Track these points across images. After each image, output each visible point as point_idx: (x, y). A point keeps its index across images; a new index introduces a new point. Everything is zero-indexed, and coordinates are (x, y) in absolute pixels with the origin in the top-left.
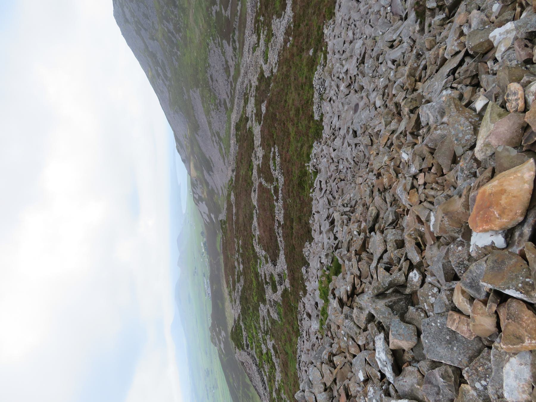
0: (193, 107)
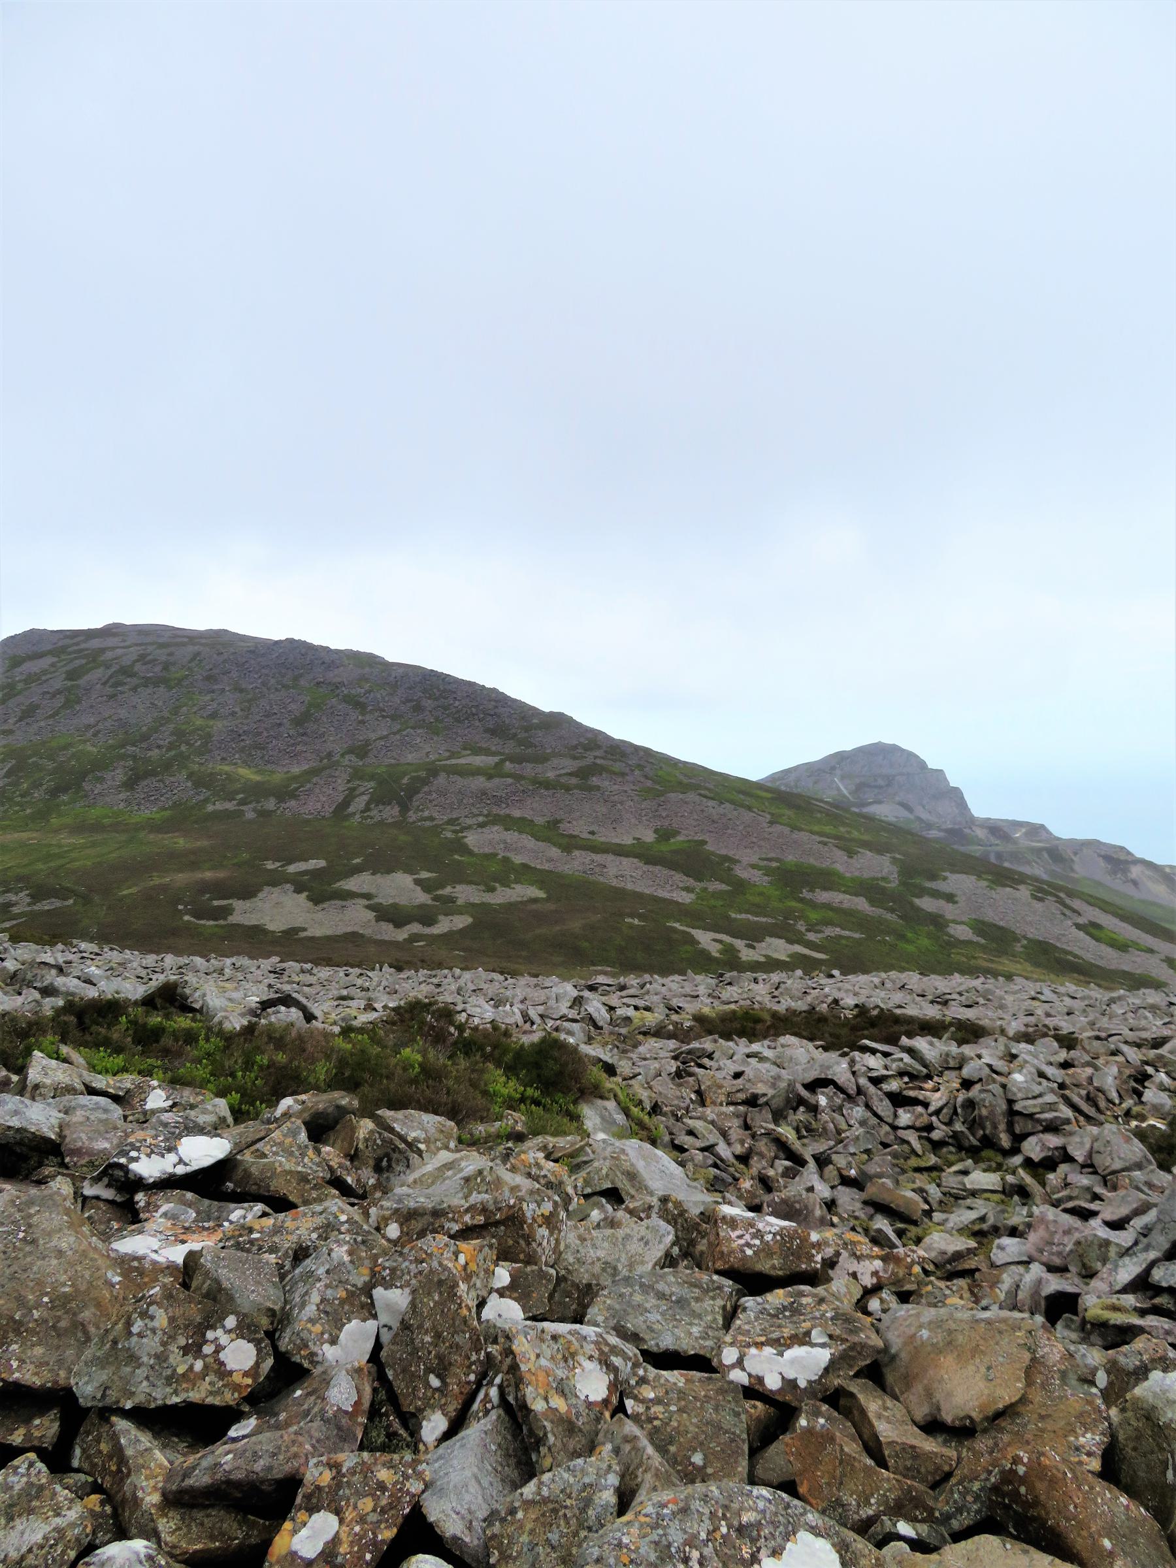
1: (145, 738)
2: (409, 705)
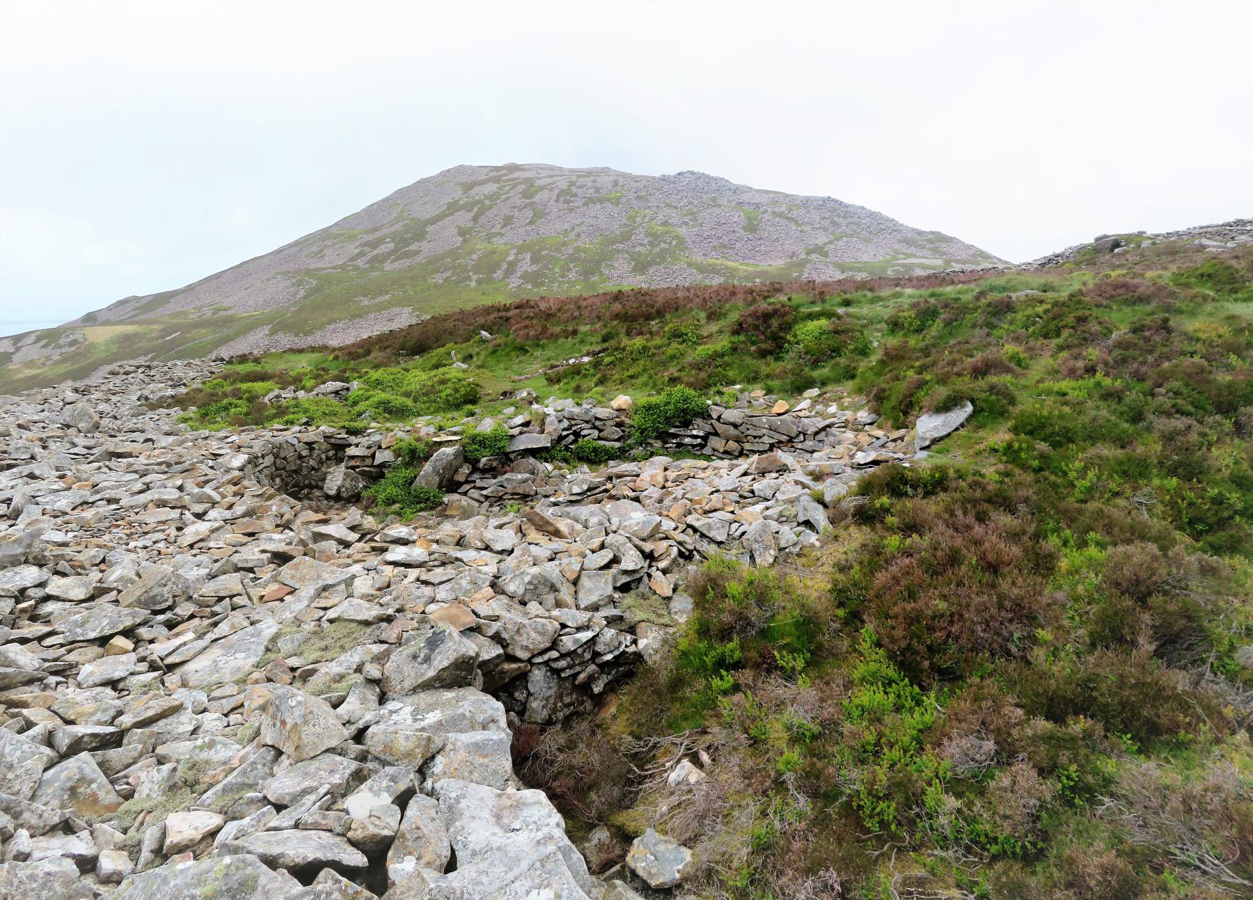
1: (625, 238)
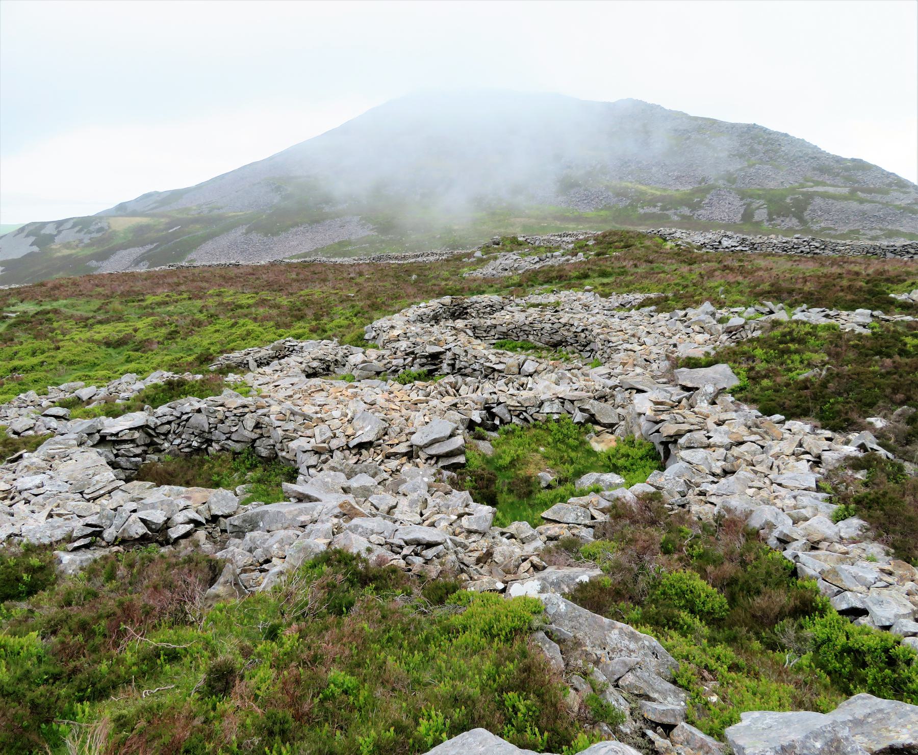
0: (317, 222)
2: (746, 148)
